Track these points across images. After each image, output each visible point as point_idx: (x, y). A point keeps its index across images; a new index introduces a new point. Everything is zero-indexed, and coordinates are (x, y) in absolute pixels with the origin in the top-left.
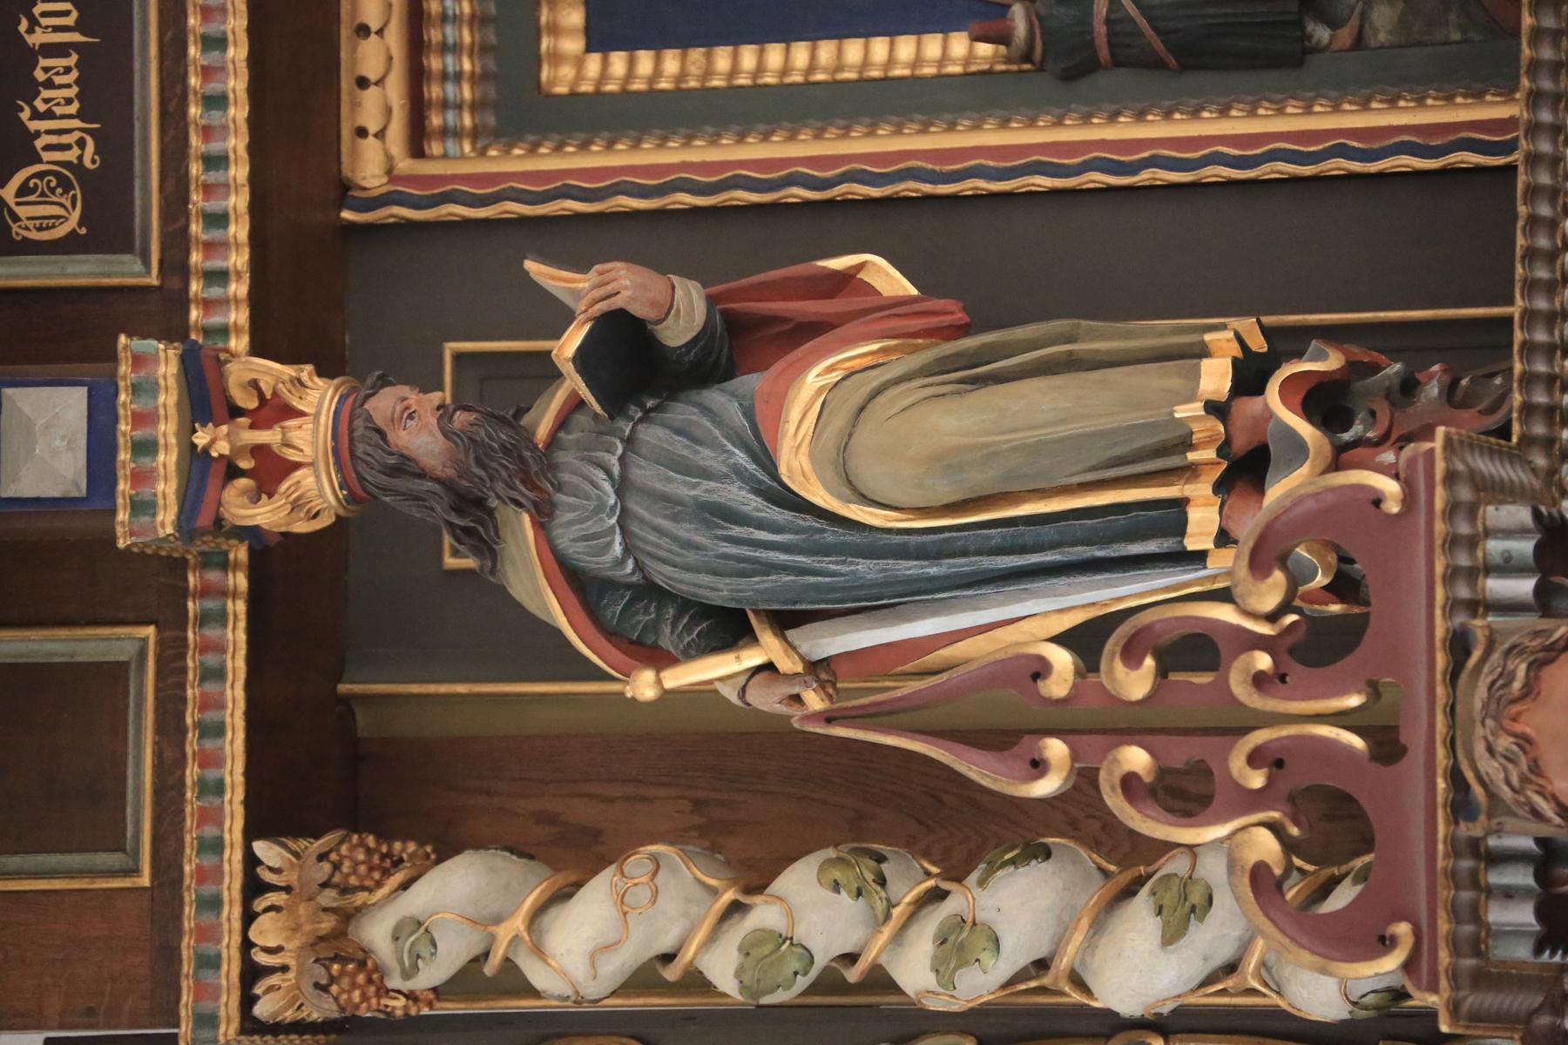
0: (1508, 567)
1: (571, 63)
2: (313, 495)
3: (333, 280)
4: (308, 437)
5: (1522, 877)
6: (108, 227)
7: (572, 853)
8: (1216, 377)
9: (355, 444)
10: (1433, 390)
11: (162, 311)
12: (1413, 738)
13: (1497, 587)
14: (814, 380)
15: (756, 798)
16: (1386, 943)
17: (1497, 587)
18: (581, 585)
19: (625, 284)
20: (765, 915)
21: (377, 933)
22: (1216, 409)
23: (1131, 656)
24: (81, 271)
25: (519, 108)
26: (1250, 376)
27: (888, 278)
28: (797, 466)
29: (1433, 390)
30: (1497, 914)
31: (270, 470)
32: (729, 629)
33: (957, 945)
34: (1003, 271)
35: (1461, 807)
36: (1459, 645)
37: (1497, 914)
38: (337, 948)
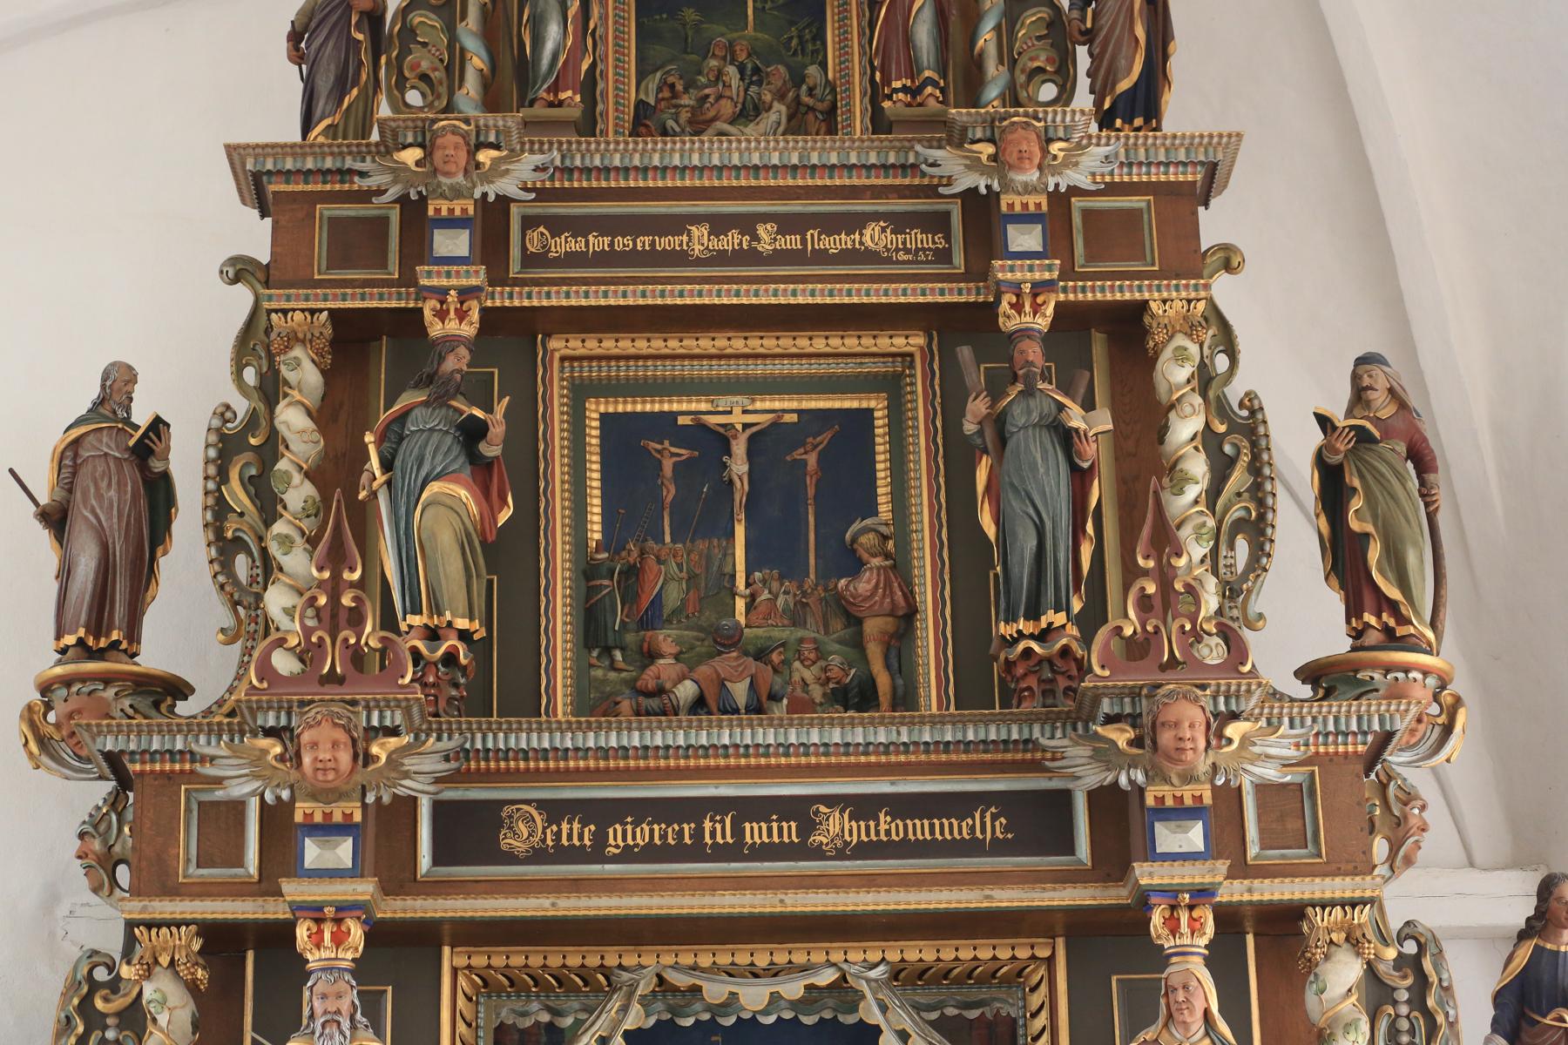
0: (381, 718)
1: (595, 409)
2: (436, 329)
3: (514, 333)
4: (452, 326)
5: (283, 722)
6: (529, 260)
7: (323, 415)
8: (462, 623)
9: (451, 342)
10: (454, 693)
11: (498, 277)
12: (327, 688)
13: (375, 714)
14: (463, 493)
15: (336, 472)
16: (261, 680)
17: (375, 714)
18: (403, 417)
19: (497, 430)
20: (297, 478)
21: (297, 352)
22: (450, 624)
23: (355, 599)
24: (515, 252)
25: (580, 392)
26: (464, 635)
27: (504, 516)
28: (434, 487)
29: (454, 693)
30: (271, 714)
31: (442, 315)
32: (387, 465)
33: (286, 541)
34: (507, 557)
35: (302, 704)
36: (354, 703)
37: (271, 714)
38: (293, 339)
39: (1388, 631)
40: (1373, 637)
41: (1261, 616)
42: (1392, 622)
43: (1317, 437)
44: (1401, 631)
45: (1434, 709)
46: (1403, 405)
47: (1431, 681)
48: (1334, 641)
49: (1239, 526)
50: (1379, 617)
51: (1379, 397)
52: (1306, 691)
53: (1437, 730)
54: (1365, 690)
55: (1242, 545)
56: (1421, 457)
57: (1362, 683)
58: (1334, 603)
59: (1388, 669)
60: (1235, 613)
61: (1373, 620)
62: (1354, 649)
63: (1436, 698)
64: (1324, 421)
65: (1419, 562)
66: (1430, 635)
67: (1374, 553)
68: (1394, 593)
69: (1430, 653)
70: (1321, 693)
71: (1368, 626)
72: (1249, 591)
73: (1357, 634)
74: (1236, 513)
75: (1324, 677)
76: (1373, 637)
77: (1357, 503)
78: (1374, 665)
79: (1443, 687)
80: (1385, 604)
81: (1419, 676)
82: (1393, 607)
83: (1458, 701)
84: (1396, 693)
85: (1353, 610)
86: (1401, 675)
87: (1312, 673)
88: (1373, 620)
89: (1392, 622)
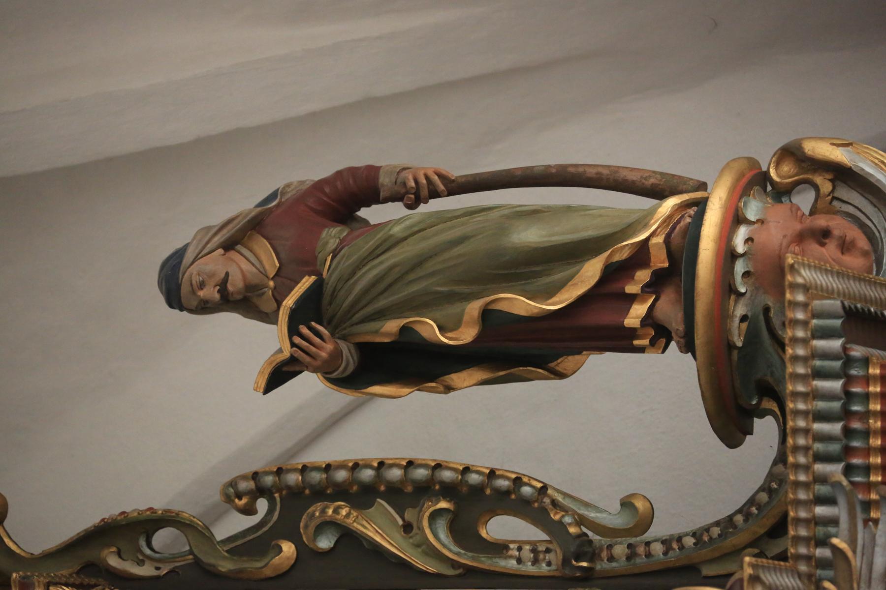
39: (656, 284)
40: (669, 309)
41: (627, 504)
42: (643, 276)
43: (308, 385)
44: (660, 260)
45: (804, 200)
46: (255, 225)
47: (753, 210)
48: (668, 381)
49: (464, 532)
50: (632, 299)
51: (240, 268)
52: (765, 429)
53: (844, 192)
54: (766, 331)
55: (501, 527)
56: (347, 197)
57: (752, 337)
58: (600, 367)
59: (726, 288)
60: (620, 550)
61: (638, 311)
62: (688, 346)
63: (781, 193)
64: (279, 375)
65: (539, 218)
66: (671, 203)
67: (519, 304)
68: (591, 271)
69: (701, 205)
70: (769, 404)
71: (648, 319)
72: (581, 521)
73: (661, 335)
74: (441, 538)
75: (738, 396)
76: (669, 309)
77: (429, 328)
78: (720, 316)
79: (761, 180)
80: (609, 290)
81: (742, 233)
82: (615, 273)
83: (790, 152)
84: (773, 274)
85: (621, 340)
86: (740, 267)
87: (731, 419)
88: (638, 311)
89: (643, 276)
